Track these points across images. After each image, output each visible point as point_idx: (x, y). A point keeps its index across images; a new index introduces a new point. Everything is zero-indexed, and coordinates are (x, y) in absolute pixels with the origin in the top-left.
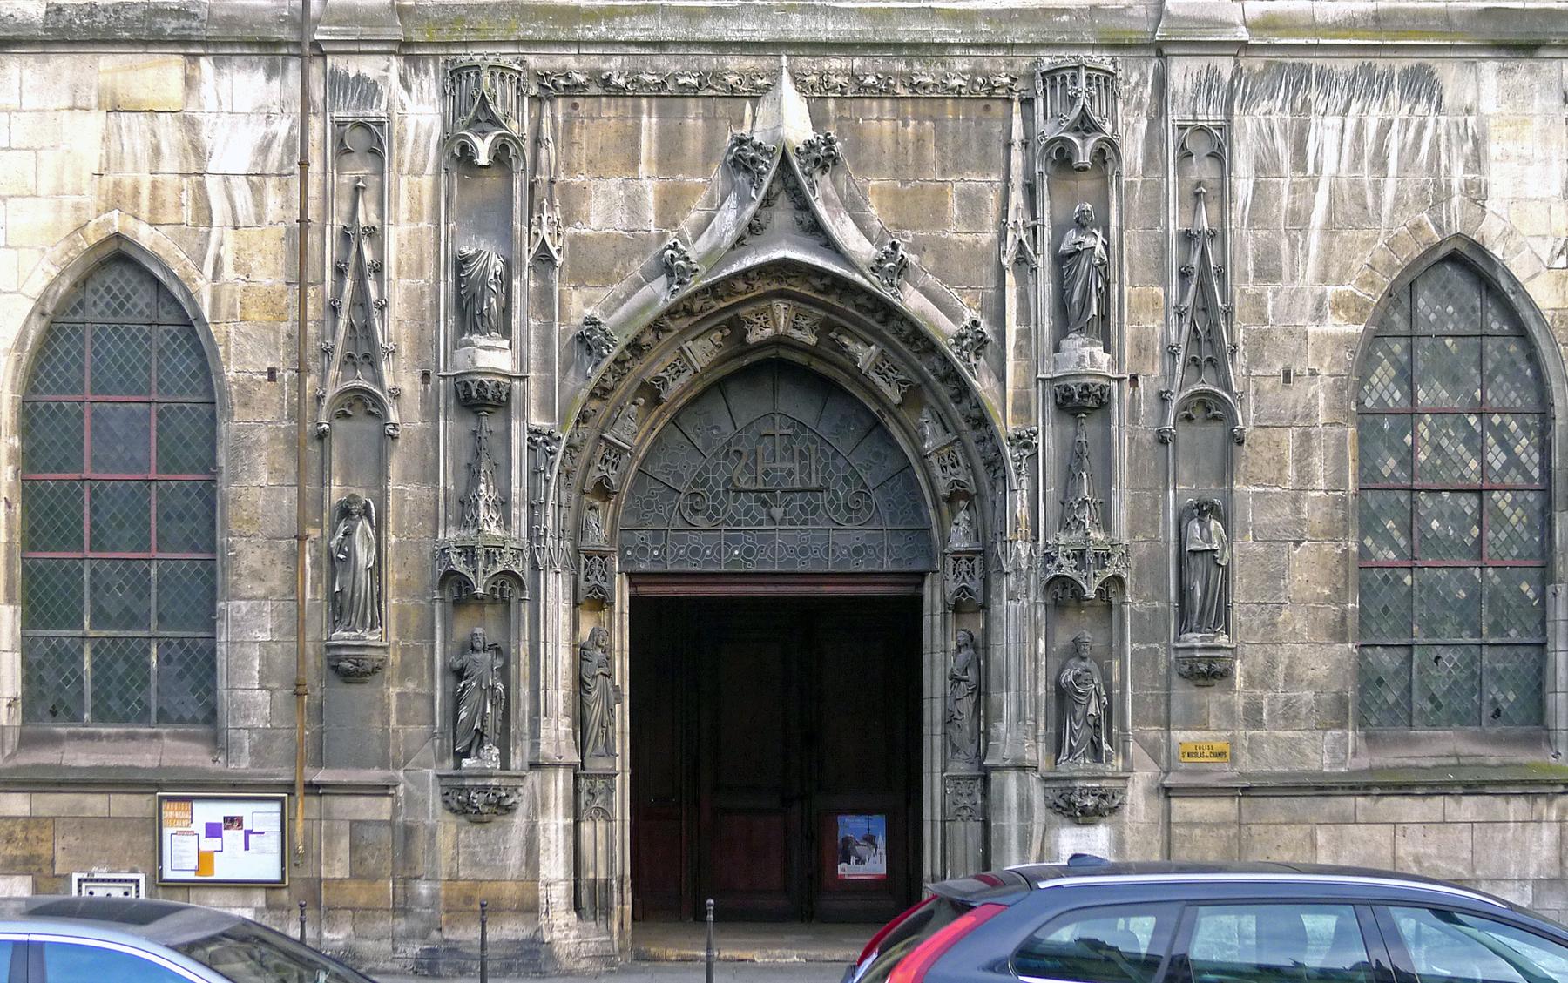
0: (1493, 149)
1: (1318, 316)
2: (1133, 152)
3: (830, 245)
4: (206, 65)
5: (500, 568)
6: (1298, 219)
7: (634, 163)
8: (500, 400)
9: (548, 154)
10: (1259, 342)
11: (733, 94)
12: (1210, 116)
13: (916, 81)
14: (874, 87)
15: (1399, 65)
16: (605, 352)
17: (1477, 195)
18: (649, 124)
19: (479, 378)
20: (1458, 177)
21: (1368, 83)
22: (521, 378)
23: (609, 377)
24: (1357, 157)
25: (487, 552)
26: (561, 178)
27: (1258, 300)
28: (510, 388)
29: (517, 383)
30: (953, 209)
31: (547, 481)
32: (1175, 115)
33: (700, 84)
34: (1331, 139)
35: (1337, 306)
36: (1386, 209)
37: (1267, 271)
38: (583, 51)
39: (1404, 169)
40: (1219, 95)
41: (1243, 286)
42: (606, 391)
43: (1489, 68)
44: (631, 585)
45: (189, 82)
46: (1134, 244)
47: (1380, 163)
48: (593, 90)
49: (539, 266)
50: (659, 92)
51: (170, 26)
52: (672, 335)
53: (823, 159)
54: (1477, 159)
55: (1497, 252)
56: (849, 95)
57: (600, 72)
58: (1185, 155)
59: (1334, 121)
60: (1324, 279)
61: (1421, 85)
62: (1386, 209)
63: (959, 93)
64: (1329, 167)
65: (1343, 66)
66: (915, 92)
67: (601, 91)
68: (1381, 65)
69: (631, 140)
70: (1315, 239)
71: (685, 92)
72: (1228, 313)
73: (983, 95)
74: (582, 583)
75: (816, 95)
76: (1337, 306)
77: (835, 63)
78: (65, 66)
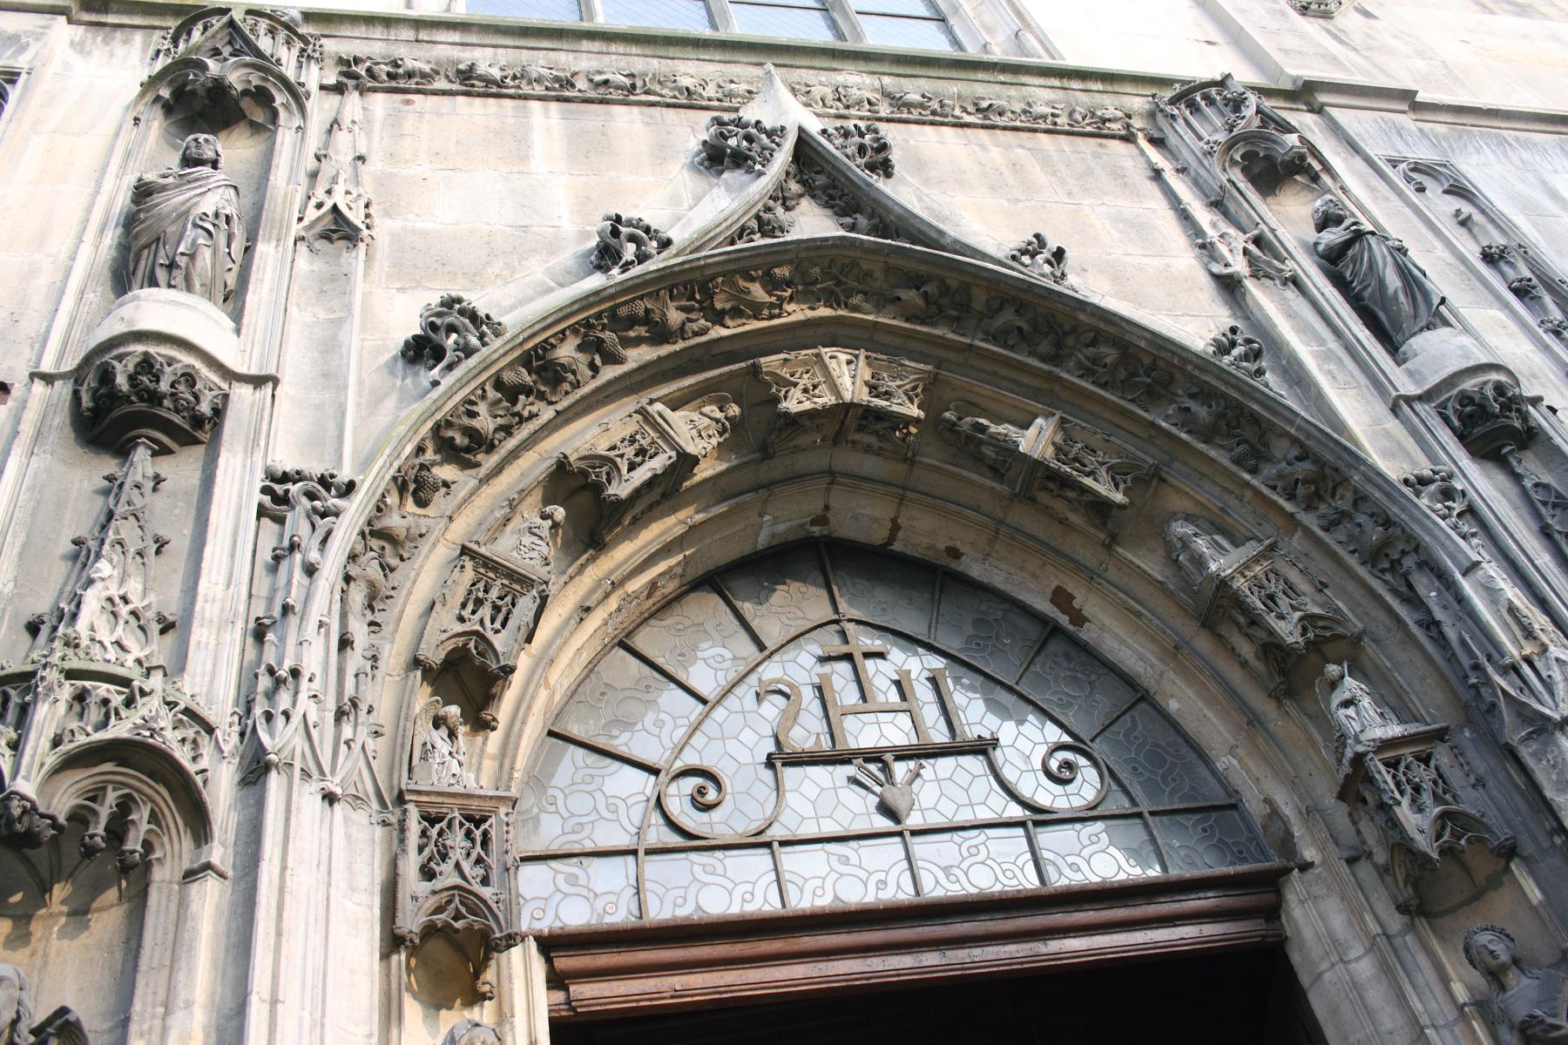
5: (119, 730)
7: (524, 158)
8: (198, 421)
13: (985, 104)
14: (922, 106)
16: (474, 341)
19: (140, 348)
22: (258, 381)
23: (482, 408)
25: (81, 697)
26: (375, 166)
28: (226, 397)
29: (242, 395)
31: (310, 570)
33: (633, 86)
38: (423, 35)
42: (480, 443)
44: (556, 981)
48: (441, 84)
49: (321, 245)
52: (617, 370)
56: (882, 114)
57: (460, 62)
63: (1055, 124)
66: (986, 118)
67: (456, 87)
73: (1089, 129)
74: (411, 880)
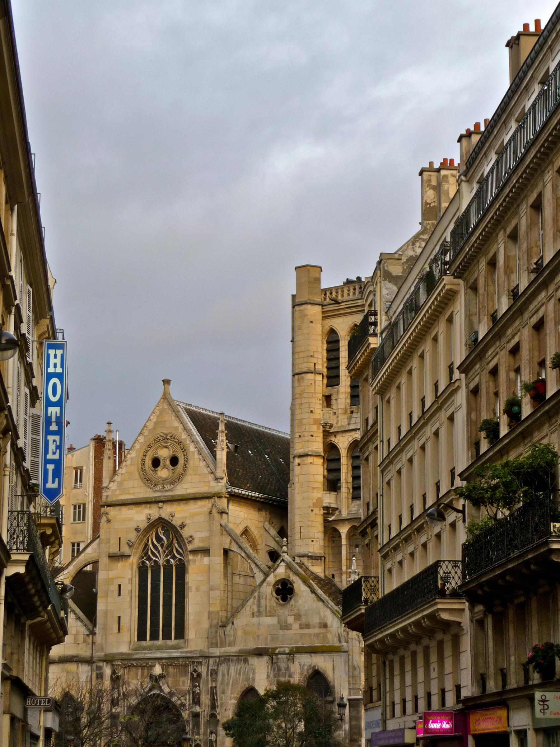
0: (256, 671)
1: (230, 700)
2: (204, 674)
3: (162, 690)
4: (80, 664)
6: (228, 684)
9: (126, 676)
10: (222, 704)
11: (151, 666)
12: (215, 668)
15: (243, 658)
17: (254, 679)
18: (140, 671)
20: (251, 676)
21: (238, 661)
24: (237, 673)
27: (222, 698)
30: (181, 683)
32: (210, 668)
34: (233, 670)
35: (233, 698)
36: (241, 681)
37: (223, 692)
39: (243, 675)
40: (217, 664)
41: (219, 695)
43: (256, 658)
45: (78, 667)
46: (204, 689)
47: (240, 674)
50: (141, 666)
51: (75, 659)
53: (162, 676)
54: (254, 673)
55: (257, 688)
58: (211, 674)
59: (233, 667)
60: (231, 694)
61: (246, 661)
62: (241, 681)
64: (233, 675)
65: (235, 658)
68: (240, 658)
69: (137, 673)
70: (230, 687)
71: (144, 666)
72: (217, 700)
75: (162, 666)
76: (233, 698)
77: (164, 661)
78: (61, 666)
